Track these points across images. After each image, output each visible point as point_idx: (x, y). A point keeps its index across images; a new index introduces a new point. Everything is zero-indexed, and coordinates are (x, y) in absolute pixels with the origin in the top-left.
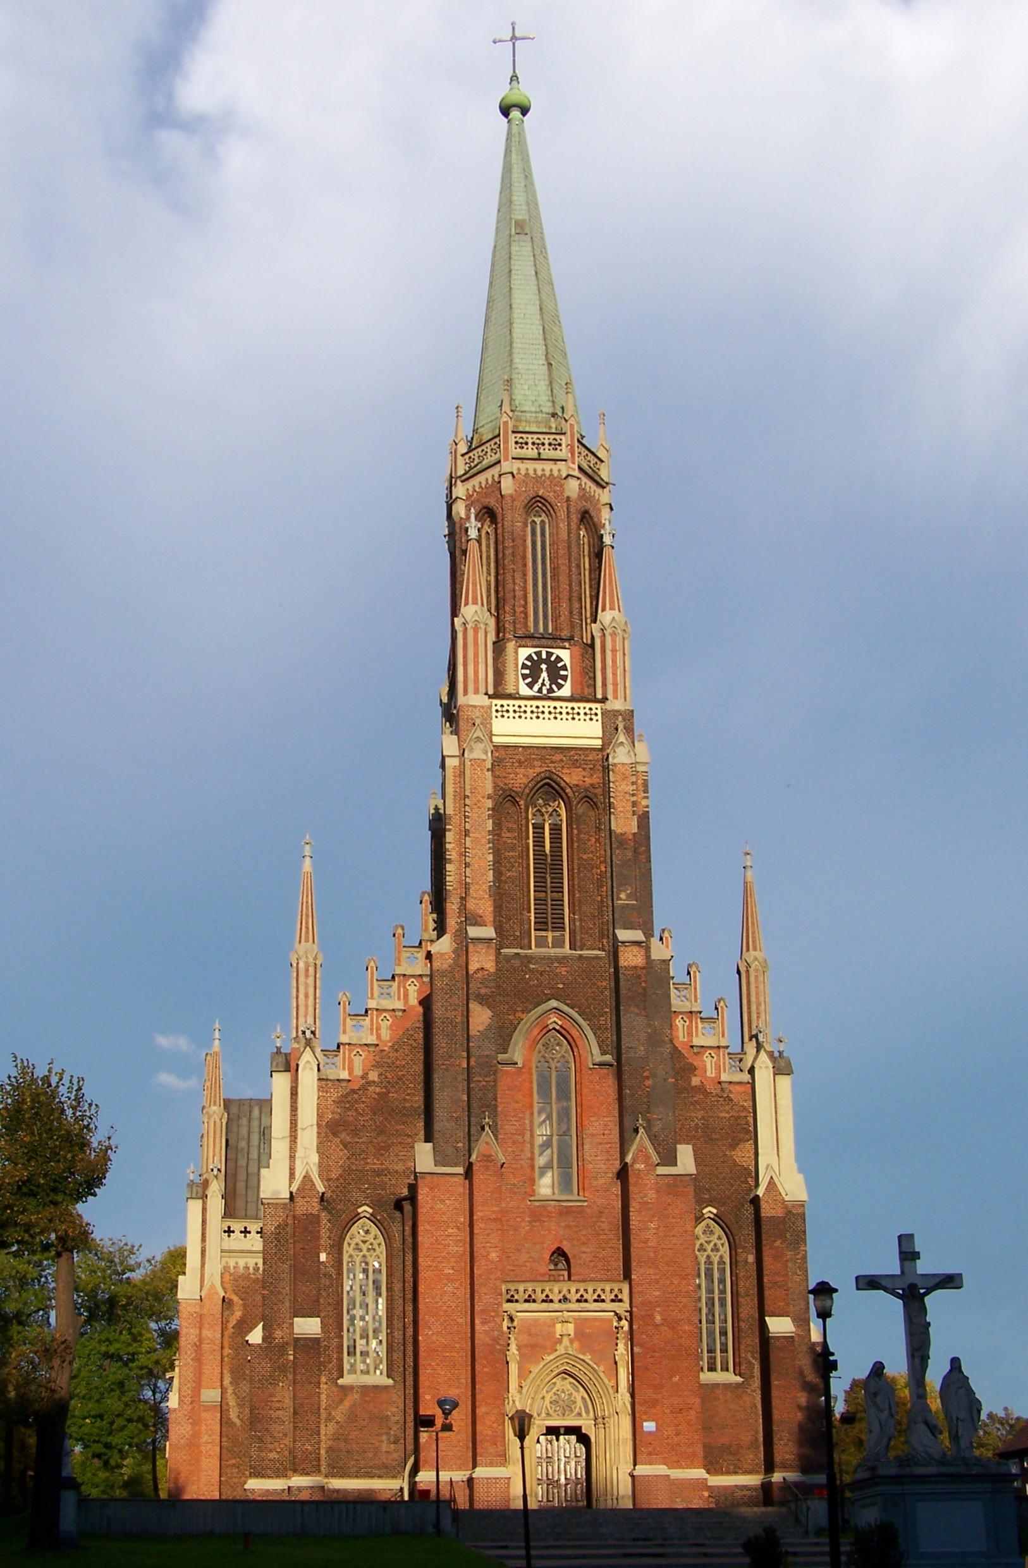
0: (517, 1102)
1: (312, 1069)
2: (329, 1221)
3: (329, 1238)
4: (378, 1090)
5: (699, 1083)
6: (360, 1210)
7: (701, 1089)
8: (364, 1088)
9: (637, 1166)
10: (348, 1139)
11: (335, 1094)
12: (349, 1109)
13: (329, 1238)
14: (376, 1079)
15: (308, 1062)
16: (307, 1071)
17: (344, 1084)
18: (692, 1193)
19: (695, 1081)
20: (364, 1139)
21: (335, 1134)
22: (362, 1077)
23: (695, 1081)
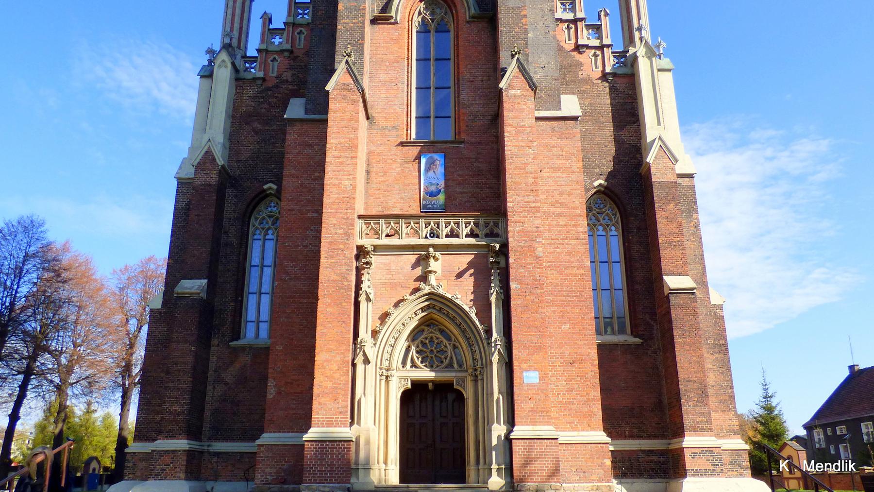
0: (392, 53)
1: (226, 67)
2: (236, 196)
3: (234, 211)
4: (290, 87)
5: (585, 76)
6: (265, 187)
7: (587, 81)
8: (277, 86)
9: (512, 92)
10: (259, 127)
11: (250, 91)
12: (262, 103)
13: (234, 211)
14: (290, 79)
15: (223, 61)
16: (223, 70)
17: (260, 82)
18: (579, 136)
19: (581, 75)
20: (275, 127)
21: (248, 123)
22: (277, 77)
23: (581, 75)
